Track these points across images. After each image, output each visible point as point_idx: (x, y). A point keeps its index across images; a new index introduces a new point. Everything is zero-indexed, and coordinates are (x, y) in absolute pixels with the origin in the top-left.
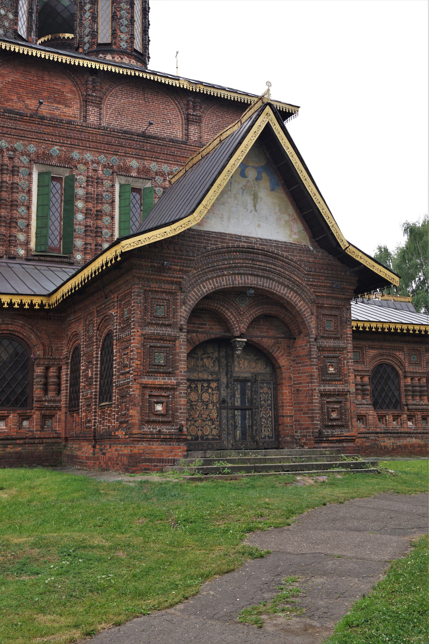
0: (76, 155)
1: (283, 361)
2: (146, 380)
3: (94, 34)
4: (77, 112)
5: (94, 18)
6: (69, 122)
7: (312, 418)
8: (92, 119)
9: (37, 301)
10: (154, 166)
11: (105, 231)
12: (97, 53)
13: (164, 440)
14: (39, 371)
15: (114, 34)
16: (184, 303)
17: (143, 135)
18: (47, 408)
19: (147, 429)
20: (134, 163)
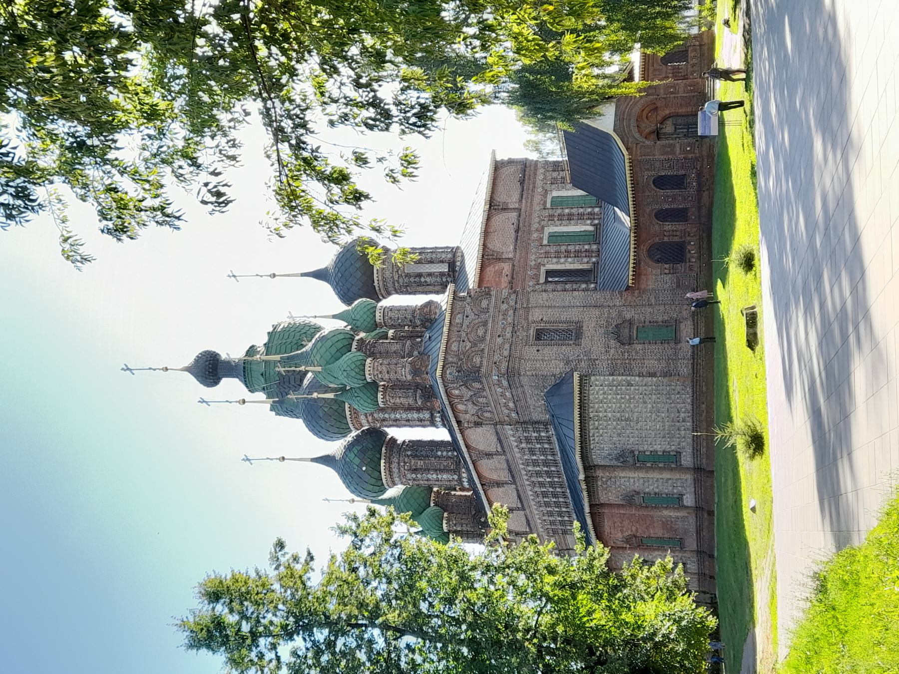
0: (533, 263)
1: (667, 112)
2: (678, 152)
3: (442, 274)
4: (507, 264)
5: (430, 275)
6: (513, 265)
7: (693, 96)
8: (511, 256)
9: (632, 235)
10: (535, 226)
11: (577, 248)
12: (454, 271)
13: (702, 146)
14: (666, 239)
15: (442, 262)
16: (644, 143)
17: (517, 231)
18: (685, 234)
19: (697, 151)
20: (535, 235)
